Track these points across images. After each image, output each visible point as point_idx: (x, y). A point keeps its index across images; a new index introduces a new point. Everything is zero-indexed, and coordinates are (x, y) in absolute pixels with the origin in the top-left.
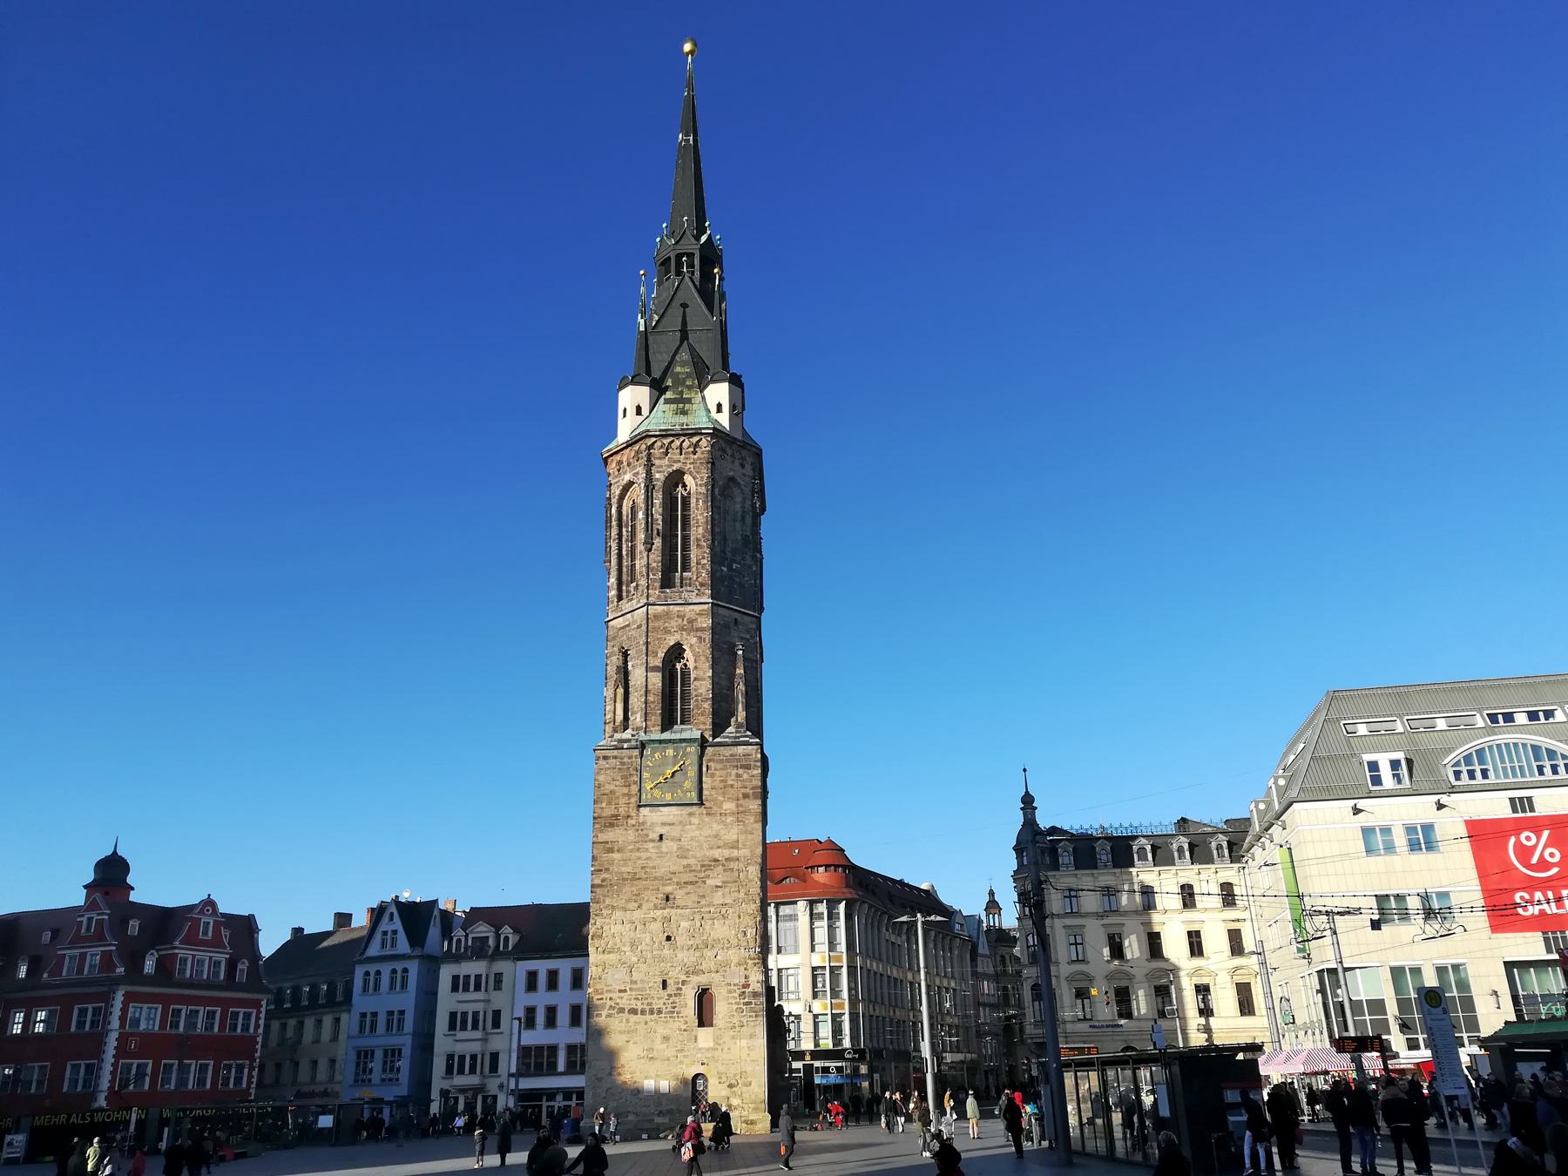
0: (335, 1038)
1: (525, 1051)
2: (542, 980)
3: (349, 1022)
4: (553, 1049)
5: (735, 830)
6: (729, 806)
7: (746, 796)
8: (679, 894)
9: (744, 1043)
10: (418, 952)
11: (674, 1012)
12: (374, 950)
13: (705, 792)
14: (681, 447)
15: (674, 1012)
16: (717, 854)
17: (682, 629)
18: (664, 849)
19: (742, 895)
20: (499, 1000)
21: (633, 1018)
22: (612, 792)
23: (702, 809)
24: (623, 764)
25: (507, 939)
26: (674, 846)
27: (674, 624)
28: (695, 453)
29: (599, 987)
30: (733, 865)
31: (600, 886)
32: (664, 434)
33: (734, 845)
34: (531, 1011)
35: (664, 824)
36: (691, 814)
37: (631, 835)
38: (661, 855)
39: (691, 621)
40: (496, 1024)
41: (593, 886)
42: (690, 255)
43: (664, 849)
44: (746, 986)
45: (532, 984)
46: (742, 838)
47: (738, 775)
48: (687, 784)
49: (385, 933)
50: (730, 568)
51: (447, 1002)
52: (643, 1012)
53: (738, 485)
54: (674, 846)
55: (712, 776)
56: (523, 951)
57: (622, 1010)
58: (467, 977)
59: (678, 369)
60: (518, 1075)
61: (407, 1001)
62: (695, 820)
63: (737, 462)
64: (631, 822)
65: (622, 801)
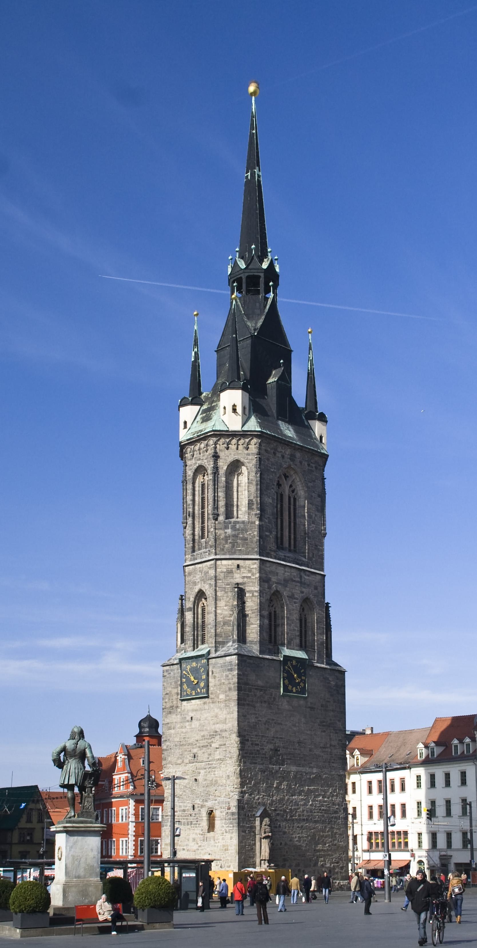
5: (225, 712)
6: (222, 697)
7: (230, 689)
8: (200, 753)
13: (211, 689)
14: (199, 449)
17: (201, 580)
18: (193, 726)
28: (207, 451)
30: (224, 734)
33: (225, 722)
35: (193, 710)
36: (205, 703)
43: (193, 726)
46: (228, 716)
48: (202, 684)
50: (234, 528)
55: (215, 677)
62: (206, 707)
64: (179, 710)
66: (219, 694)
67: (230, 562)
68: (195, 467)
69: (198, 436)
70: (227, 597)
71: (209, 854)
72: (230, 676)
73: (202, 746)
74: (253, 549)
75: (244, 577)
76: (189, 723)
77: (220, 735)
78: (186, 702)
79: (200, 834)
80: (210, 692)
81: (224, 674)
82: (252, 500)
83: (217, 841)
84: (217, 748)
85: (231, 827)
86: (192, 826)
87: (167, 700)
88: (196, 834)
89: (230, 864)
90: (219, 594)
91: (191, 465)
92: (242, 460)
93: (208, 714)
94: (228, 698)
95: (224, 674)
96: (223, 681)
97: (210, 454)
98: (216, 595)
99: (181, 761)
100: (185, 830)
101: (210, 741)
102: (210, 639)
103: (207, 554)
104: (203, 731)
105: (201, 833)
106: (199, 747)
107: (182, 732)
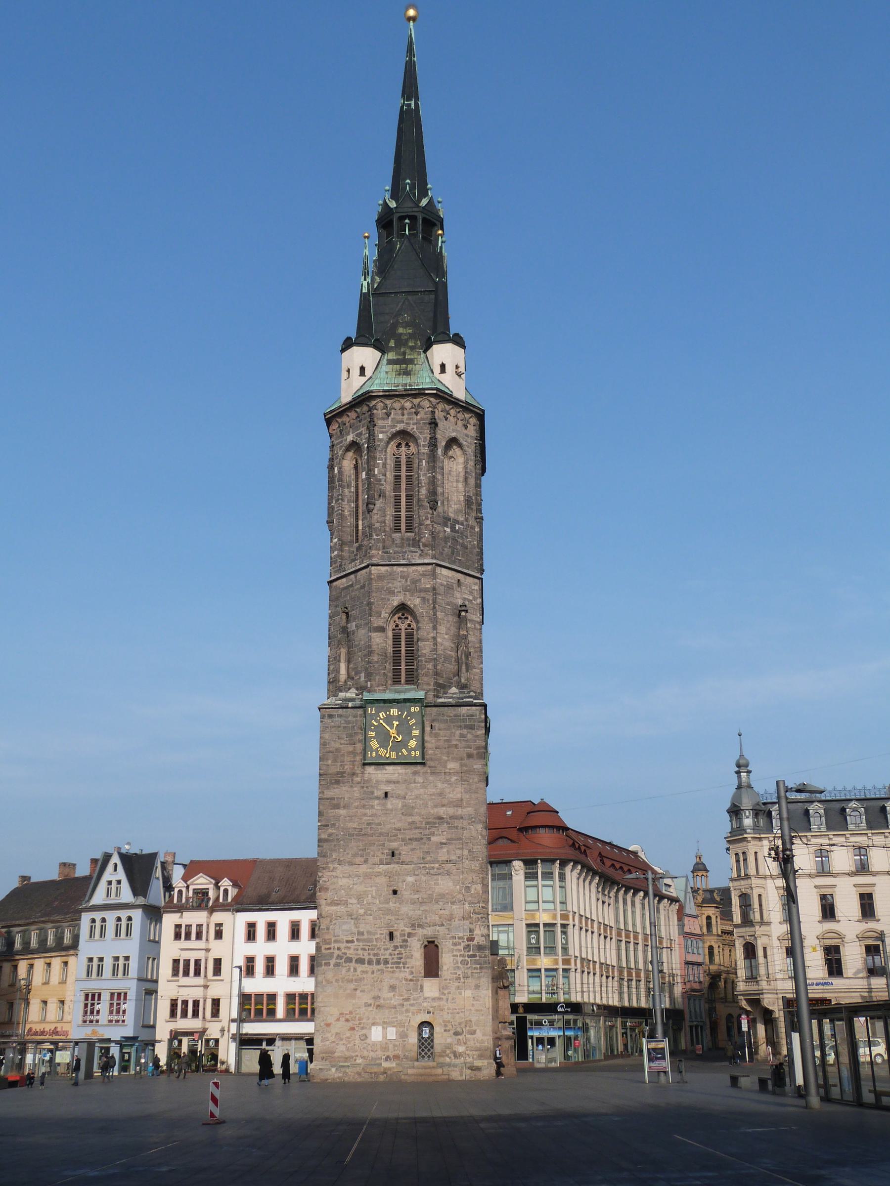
0: (63, 982)
1: (245, 998)
2: (261, 931)
3: (77, 964)
4: (272, 997)
5: (459, 789)
6: (452, 765)
7: (470, 756)
8: (405, 852)
9: (469, 993)
10: (141, 900)
11: (400, 963)
12: (99, 897)
15: (400, 963)
16: (441, 811)
17: (406, 590)
18: (389, 806)
19: (466, 852)
20: (218, 949)
21: (360, 968)
22: (338, 750)
23: (425, 769)
24: (348, 722)
25: (226, 891)
26: (399, 804)
27: (398, 584)
29: (327, 937)
30: (457, 823)
31: (326, 841)
32: (389, 395)
33: (459, 804)
34: (250, 960)
35: (389, 782)
36: (415, 773)
37: (357, 792)
38: (386, 812)
39: (415, 582)
40: (217, 970)
41: (320, 841)
42: (413, 218)
43: (389, 806)
44: (471, 939)
45: (251, 935)
47: (462, 736)
48: (413, 743)
49: (110, 883)
50: (453, 529)
51: (170, 949)
52: (370, 962)
53: (460, 446)
54: (399, 804)
55: (436, 735)
56: (239, 905)
57: (349, 960)
58: (189, 926)
59: (401, 330)
60: (241, 1020)
61: (131, 947)
62: (420, 779)
63: (460, 423)
65: (347, 759)
66: (446, 762)
67: (450, 573)
68: (394, 430)
69: (406, 390)
70: (448, 621)
71: (429, 1012)
72: (469, 736)
73: (410, 839)
74: (474, 562)
75: (465, 599)
76: (384, 801)
77: (448, 823)
78: (373, 767)
79: (406, 980)
80: (427, 757)
81: (458, 732)
82: (469, 497)
83: (446, 992)
84: (442, 844)
85: (475, 968)
86: (389, 966)
87: (330, 762)
88: (397, 978)
89: (474, 1028)
90: (440, 615)
91: (384, 427)
92: (461, 441)
93: (422, 791)
94: (465, 768)
95: (458, 732)
96: (454, 742)
97: (422, 419)
98: (435, 614)
99: (363, 860)
100: (373, 973)
101: (427, 832)
102: (426, 679)
103: (418, 554)
104: (411, 815)
105: (410, 977)
106: (403, 840)
107: (365, 815)
